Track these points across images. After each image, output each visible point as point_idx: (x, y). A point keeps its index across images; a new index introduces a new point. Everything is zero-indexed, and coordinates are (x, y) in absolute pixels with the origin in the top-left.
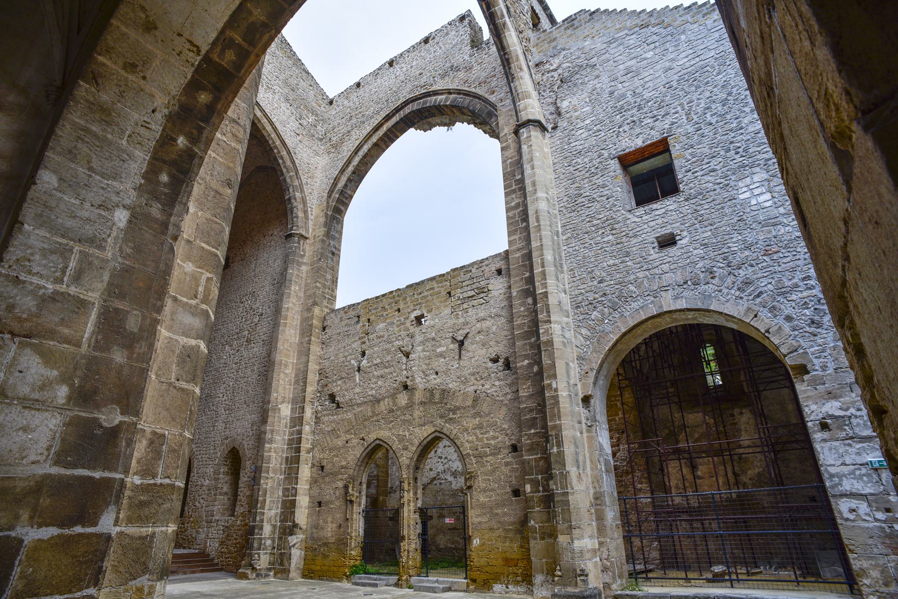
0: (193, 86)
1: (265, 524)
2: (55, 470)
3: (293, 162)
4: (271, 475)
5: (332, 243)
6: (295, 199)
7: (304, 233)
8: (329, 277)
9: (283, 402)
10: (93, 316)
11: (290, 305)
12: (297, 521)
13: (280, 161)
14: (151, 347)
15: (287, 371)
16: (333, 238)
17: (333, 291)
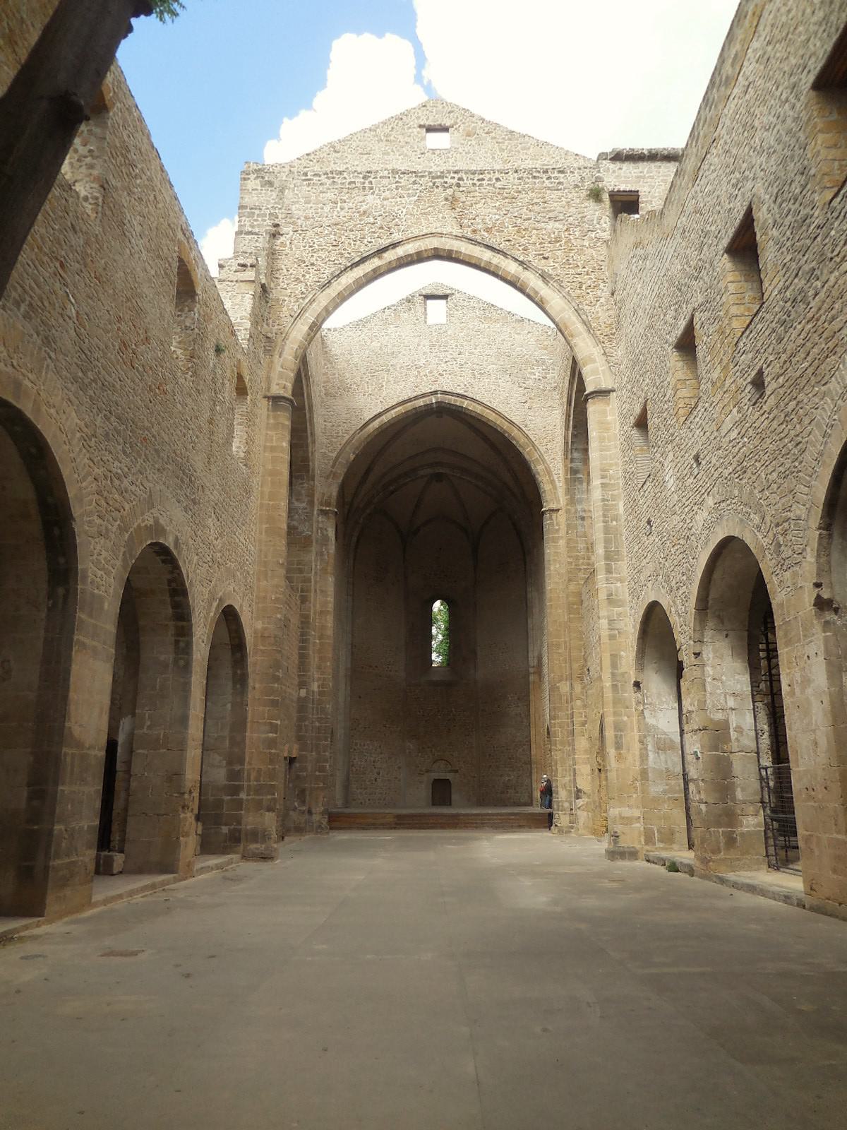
0: (233, 653)
1: (560, 789)
2: (227, 783)
3: (527, 437)
4: (559, 747)
5: (579, 507)
6: (539, 474)
7: (554, 506)
8: (581, 546)
9: (561, 681)
10: (227, 741)
11: (552, 585)
12: (579, 787)
13: (514, 442)
14: (245, 744)
15: (560, 651)
16: (580, 501)
17: (589, 558)
